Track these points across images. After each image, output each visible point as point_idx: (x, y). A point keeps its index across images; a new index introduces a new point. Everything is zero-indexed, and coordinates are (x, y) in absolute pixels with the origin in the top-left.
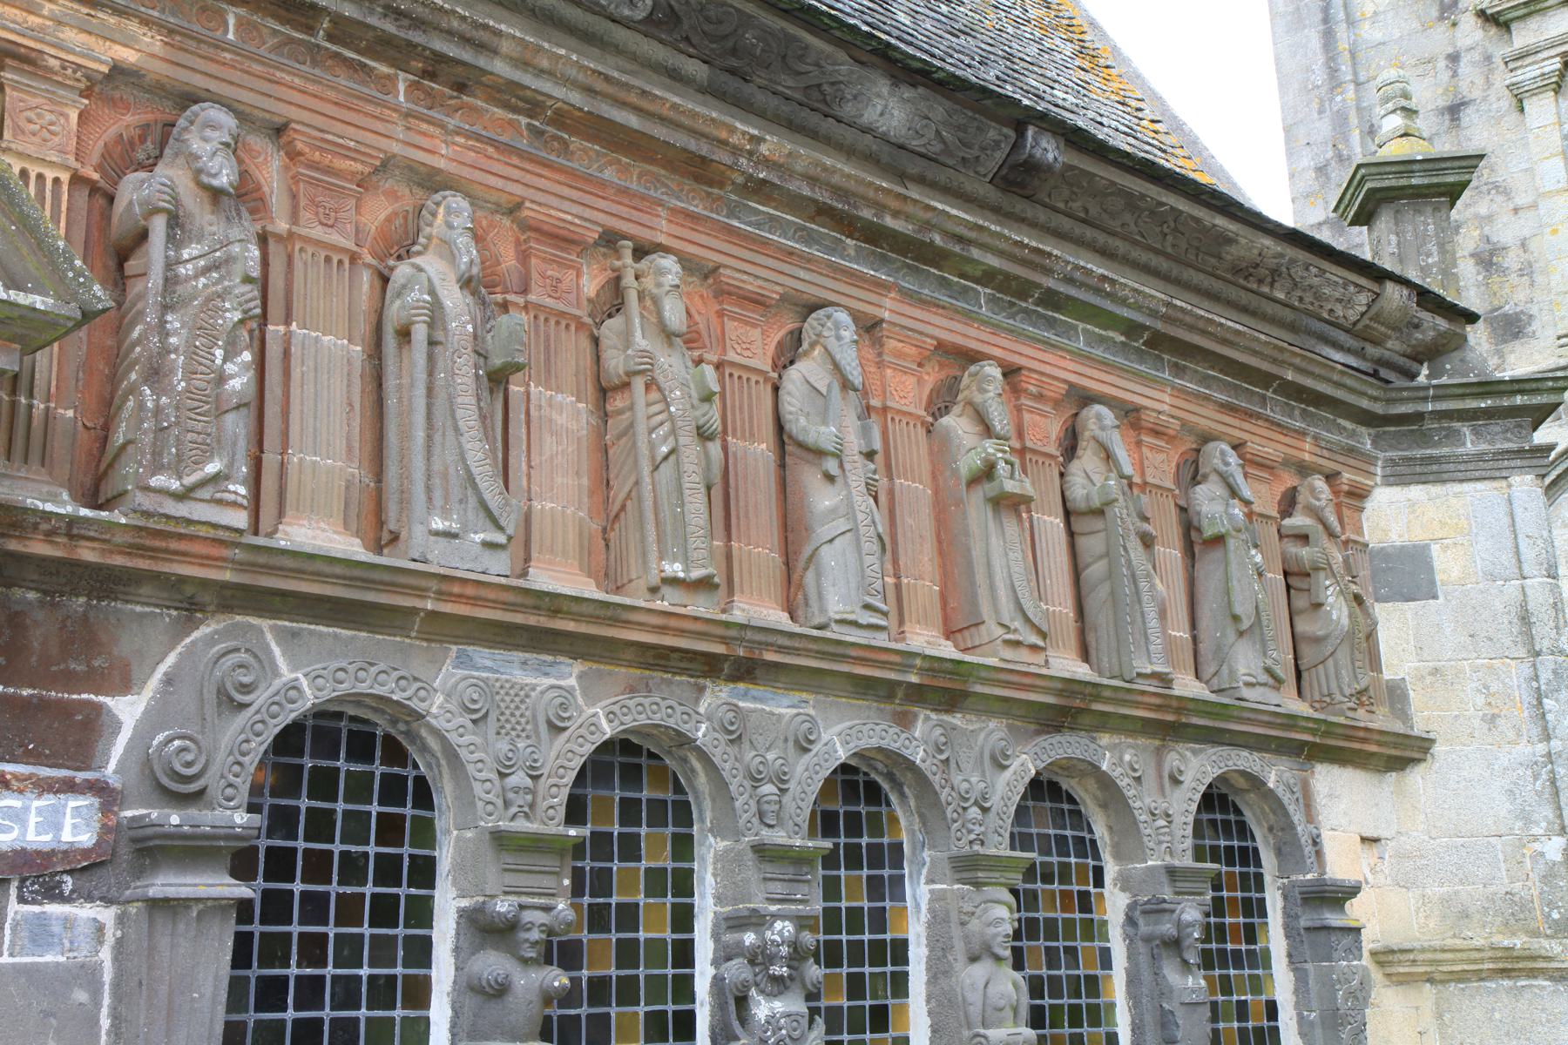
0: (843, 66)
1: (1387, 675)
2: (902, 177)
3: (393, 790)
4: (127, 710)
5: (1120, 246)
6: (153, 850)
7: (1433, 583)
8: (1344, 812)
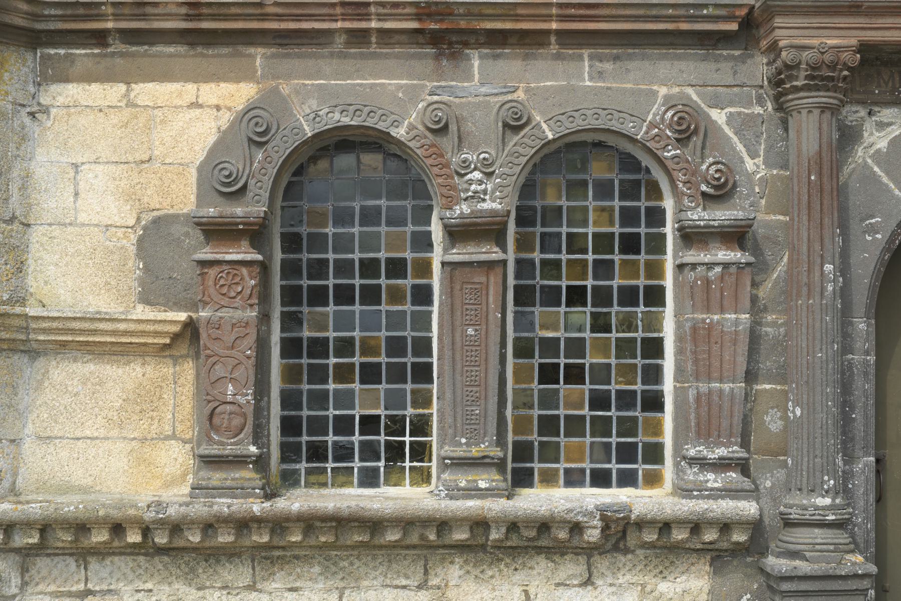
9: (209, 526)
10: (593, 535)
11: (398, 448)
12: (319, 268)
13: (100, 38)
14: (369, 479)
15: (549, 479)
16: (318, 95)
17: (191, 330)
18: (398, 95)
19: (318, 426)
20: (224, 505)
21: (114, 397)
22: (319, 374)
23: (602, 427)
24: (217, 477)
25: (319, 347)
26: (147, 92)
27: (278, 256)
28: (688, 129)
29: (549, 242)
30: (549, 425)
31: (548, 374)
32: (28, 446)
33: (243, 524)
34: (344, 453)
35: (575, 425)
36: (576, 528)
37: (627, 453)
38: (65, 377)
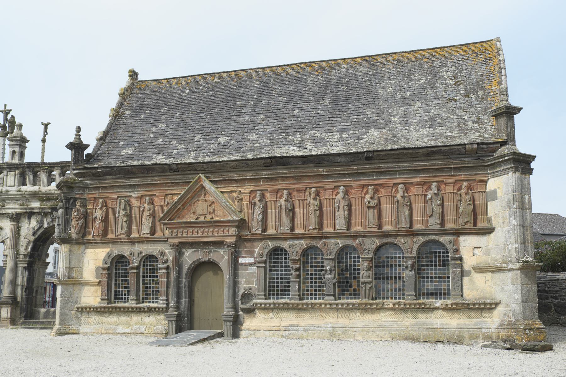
0: (331, 158)
1: (489, 216)
2: (350, 166)
3: (286, 255)
4: (257, 250)
5: (397, 160)
6: (260, 262)
7: (497, 196)
8: (467, 243)
9: (101, 308)
10: (146, 309)
11: (126, 298)
12: (119, 273)
13: (92, 243)
14: (125, 302)
15: (146, 302)
16: (118, 250)
17: (100, 281)
18: (126, 250)
19: (119, 295)
20: (102, 305)
21: (92, 291)
22: (119, 288)
23: (153, 295)
24: (102, 302)
25: (119, 284)
26: (97, 250)
27: (114, 271)
28: (162, 253)
29: (147, 269)
30: (146, 295)
31: (147, 287)
32: (82, 298)
33: (104, 308)
34: (122, 299)
35: (150, 295)
36: (144, 309)
37: (156, 299)
38: (87, 288)
